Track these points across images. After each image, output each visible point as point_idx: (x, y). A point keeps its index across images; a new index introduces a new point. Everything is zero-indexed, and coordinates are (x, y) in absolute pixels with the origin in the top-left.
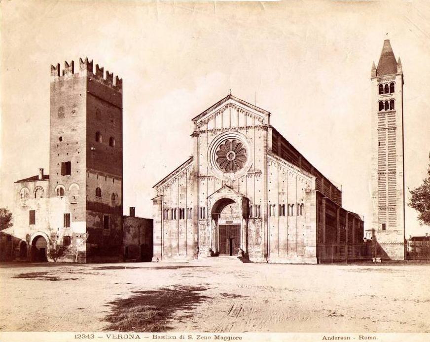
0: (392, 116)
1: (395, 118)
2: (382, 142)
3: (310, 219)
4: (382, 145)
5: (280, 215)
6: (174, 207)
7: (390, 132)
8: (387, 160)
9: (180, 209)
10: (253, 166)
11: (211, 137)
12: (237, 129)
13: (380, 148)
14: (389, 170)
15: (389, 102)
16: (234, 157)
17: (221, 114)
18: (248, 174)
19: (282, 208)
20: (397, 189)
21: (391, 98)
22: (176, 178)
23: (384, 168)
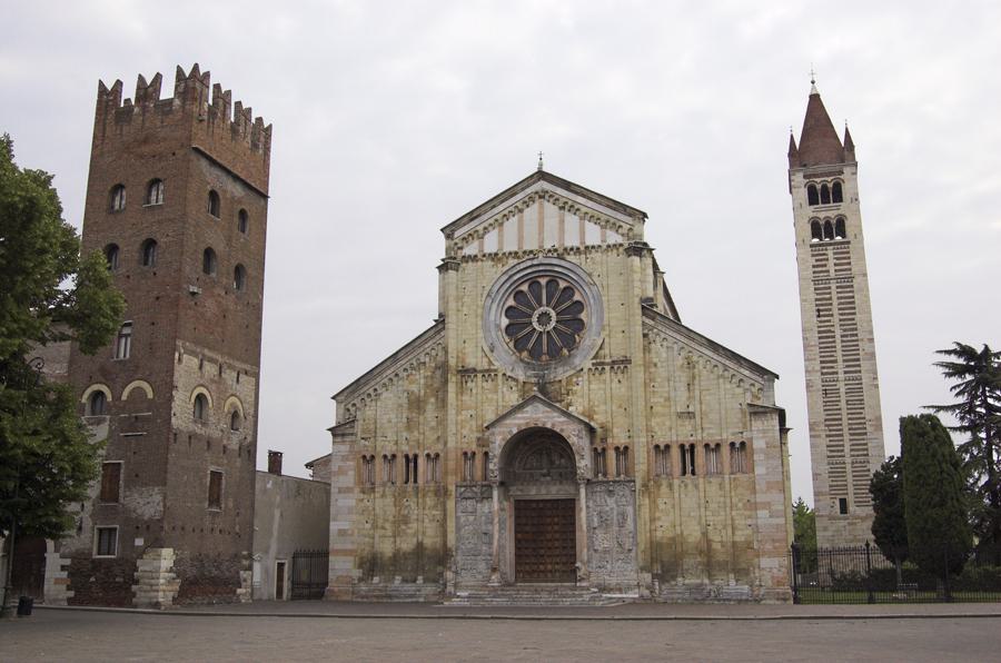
1: (849, 258)
2: (826, 310)
4: (824, 316)
5: (684, 473)
6: (389, 449)
9: (407, 457)
10: (606, 345)
11: (492, 274)
12: (561, 251)
13: (821, 322)
14: (846, 372)
16: (553, 324)
18: (593, 364)
20: (867, 417)
21: (836, 213)
22: (397, 375)
23: (832, 367)
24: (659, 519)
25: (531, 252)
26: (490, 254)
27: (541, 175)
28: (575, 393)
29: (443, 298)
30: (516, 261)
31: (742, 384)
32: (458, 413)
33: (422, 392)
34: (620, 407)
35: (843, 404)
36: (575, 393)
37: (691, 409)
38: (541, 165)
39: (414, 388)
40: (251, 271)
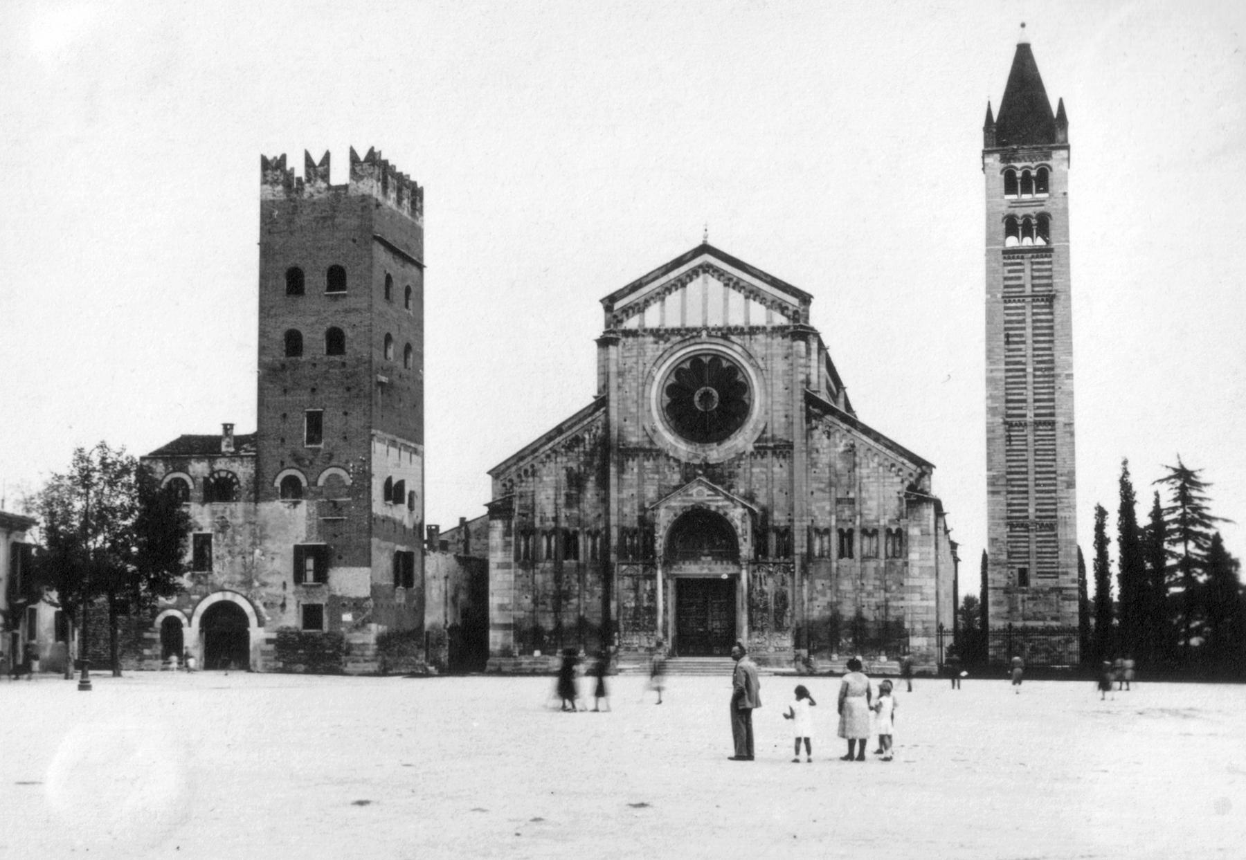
0: (1043, 263)
2: (1016, 335)
3: (921, 568)
7: (1037, 307)
8: (1030, 387)
13: (1010, 350)
15: (1034, 221)
17: (680, 291)
19: (846, 537)
24: (816, 599)
25: (695, 329)
26: (652, 330)
27: (705, 249)
28: (736, 476)
29: (604, 374)
30: (679, 338)
31: (901, 473)
32: (620, 491)
33: (582, 468)
34: (781, 491)
35: (1030, 456)
36: (736, 476)
37: (851, 495)
38: (706, 237)
39: (573, 465)
40: (414, 347)
